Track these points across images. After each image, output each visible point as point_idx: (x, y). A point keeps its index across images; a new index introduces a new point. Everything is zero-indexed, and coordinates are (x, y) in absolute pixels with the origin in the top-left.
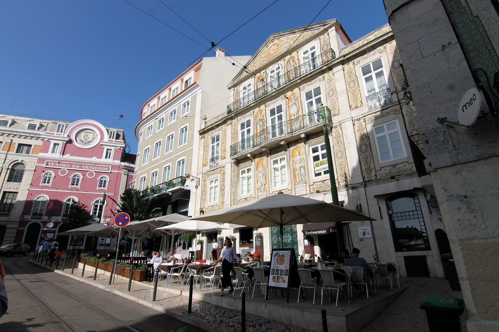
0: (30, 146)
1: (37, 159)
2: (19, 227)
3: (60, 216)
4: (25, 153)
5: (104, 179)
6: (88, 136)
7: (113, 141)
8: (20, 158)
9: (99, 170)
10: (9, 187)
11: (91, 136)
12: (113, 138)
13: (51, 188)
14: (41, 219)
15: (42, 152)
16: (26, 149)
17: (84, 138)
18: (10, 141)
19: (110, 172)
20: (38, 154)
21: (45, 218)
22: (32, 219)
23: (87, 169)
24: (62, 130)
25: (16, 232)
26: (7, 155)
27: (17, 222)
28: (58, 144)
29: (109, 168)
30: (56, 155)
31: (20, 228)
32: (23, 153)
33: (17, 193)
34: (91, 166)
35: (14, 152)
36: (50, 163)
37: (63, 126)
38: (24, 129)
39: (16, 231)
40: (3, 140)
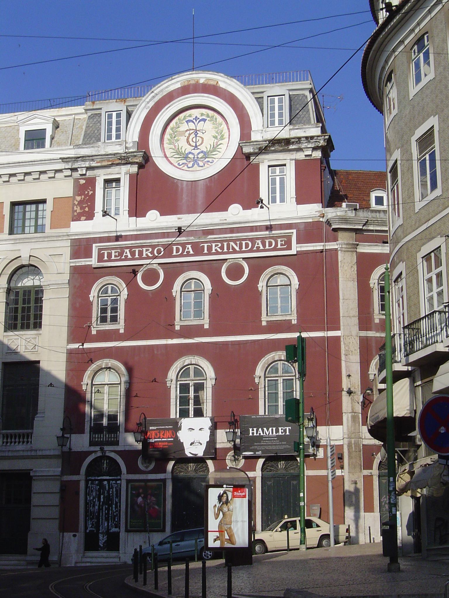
1: (68, 243)
2: (63, 473)
6: (200, 134)
9: (258, 250)
17: (188, 141)
19: (293, 252)
22: (92, 444)
23: (217, 253)
24: (118, 130)
25: (57, 490)
31: (66, 478)
32: (27, 230)
37: (119, 116)
38: (15, 148)
39: (56, 487)
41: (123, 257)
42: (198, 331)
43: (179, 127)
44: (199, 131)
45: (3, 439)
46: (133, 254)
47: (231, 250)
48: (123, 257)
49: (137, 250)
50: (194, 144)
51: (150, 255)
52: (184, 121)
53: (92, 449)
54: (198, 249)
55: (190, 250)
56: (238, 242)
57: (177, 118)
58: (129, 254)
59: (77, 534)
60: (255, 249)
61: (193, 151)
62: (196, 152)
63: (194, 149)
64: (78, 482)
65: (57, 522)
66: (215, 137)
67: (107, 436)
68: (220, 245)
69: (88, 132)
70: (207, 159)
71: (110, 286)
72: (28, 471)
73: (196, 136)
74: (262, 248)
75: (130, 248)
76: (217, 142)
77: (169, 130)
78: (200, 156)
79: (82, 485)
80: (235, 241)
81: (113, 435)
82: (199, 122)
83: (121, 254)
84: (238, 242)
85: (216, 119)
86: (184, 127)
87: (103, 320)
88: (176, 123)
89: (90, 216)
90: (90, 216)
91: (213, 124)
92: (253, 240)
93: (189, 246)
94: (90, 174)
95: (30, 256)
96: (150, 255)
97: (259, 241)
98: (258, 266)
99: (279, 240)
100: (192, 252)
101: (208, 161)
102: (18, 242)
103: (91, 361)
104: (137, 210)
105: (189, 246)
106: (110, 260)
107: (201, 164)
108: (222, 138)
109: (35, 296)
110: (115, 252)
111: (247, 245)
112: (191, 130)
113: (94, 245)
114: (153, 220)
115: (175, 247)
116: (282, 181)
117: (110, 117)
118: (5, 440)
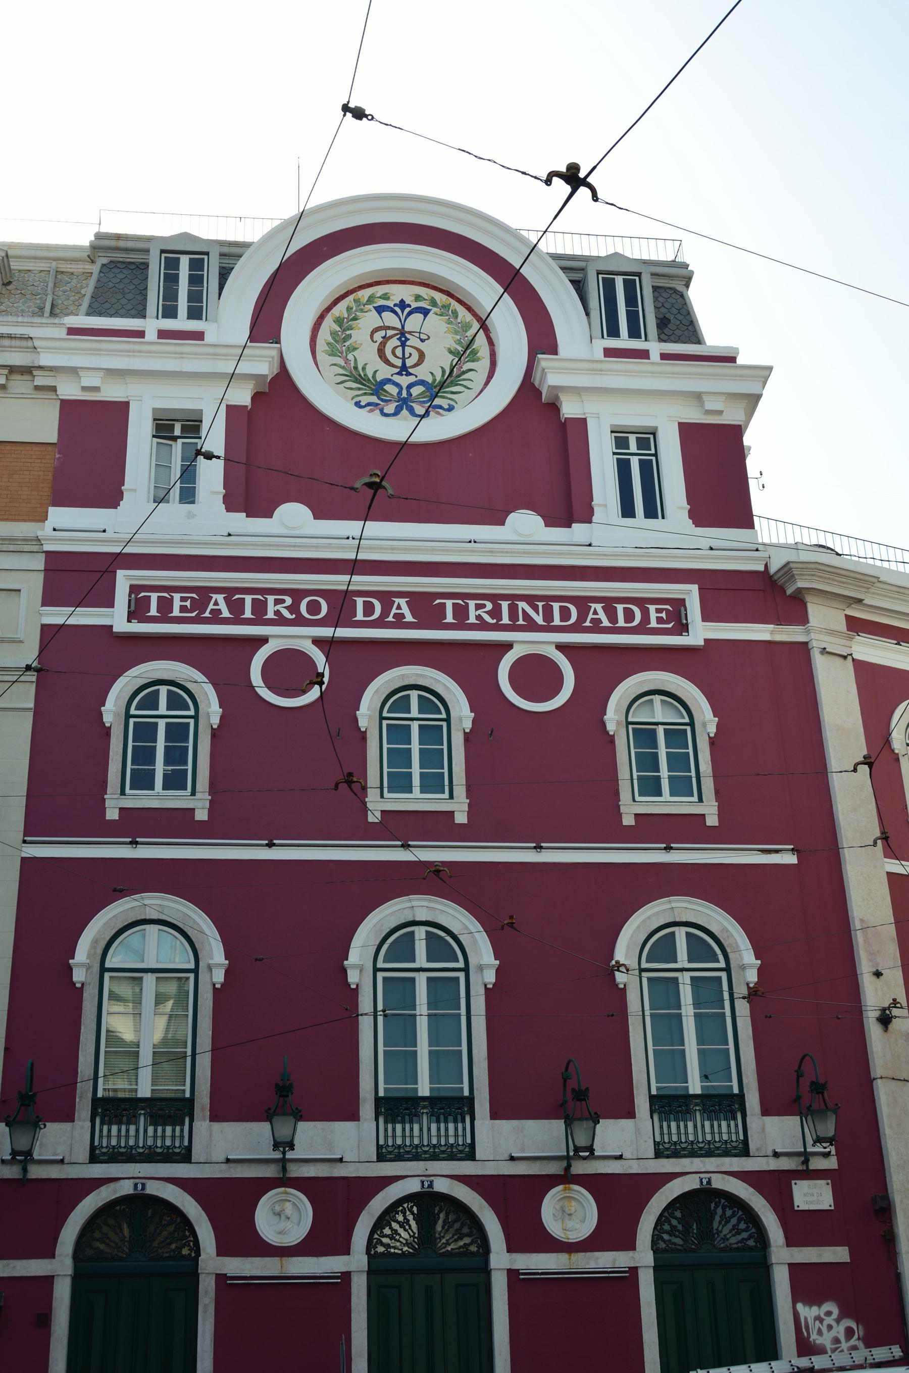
1: (39, 563)
5: (659, 713)
6: (413, 341)
9: (597, 627)
12: (634, 333)
13: (216, 828)
14: (186, 1156)
15: (66, 496)
20: (43, 518)
21: (226, 1145)
23: (482, 626)
28: (193, 426)
29: (679, 605)
30: (191, 515)
34: (513, 598)
36: (154, 597)
41: (207, 614)
42: (436, 826)
43: (355, 319)
44: (410, 333)
46: (236, 607)
48: (207, 614)
49: (248, 599)
50: (399, 363)
51: (286, 614)
52: (370, 307)
55: (406, 610)
57: (351, 298)
58: (223, 606)
60: (588, 624)
61: (397, 378)
62: (404, 381)
63: (400, 374)
64: (48, 1281)
67: (151, 1129)
68: (489, 606)
71: (163, 690)
73: (403, 345)
74: (606, 623)
75: (229, 592)
77: (328, 323)
78: (416, 391)
79: (62, 1292)
81: (160, 1129)
82: (410, 313)
85: (455, 314)
86: (370, 319)
87: (143, 781)
88: (349, 309)
89: (108, 494)
90: (108, 494)
91: (449, 322)
92: (583, 603)
93: (403, 602)
94: (112, 392)
96: (286, 614)
97: (599, 607)
98: (602, 667)
99: (652, 608)
100: (409, 618)
101: (441, 407)
103: (119, 893)
104: (250, 494)
105: (403, 602)
106: (165, 616)
107: (420, 410)
110: (183, 599)
112: (389, 328)
113: (121, 574)
114: (294, 526)
115: (360, 601)
116: (647, 469)
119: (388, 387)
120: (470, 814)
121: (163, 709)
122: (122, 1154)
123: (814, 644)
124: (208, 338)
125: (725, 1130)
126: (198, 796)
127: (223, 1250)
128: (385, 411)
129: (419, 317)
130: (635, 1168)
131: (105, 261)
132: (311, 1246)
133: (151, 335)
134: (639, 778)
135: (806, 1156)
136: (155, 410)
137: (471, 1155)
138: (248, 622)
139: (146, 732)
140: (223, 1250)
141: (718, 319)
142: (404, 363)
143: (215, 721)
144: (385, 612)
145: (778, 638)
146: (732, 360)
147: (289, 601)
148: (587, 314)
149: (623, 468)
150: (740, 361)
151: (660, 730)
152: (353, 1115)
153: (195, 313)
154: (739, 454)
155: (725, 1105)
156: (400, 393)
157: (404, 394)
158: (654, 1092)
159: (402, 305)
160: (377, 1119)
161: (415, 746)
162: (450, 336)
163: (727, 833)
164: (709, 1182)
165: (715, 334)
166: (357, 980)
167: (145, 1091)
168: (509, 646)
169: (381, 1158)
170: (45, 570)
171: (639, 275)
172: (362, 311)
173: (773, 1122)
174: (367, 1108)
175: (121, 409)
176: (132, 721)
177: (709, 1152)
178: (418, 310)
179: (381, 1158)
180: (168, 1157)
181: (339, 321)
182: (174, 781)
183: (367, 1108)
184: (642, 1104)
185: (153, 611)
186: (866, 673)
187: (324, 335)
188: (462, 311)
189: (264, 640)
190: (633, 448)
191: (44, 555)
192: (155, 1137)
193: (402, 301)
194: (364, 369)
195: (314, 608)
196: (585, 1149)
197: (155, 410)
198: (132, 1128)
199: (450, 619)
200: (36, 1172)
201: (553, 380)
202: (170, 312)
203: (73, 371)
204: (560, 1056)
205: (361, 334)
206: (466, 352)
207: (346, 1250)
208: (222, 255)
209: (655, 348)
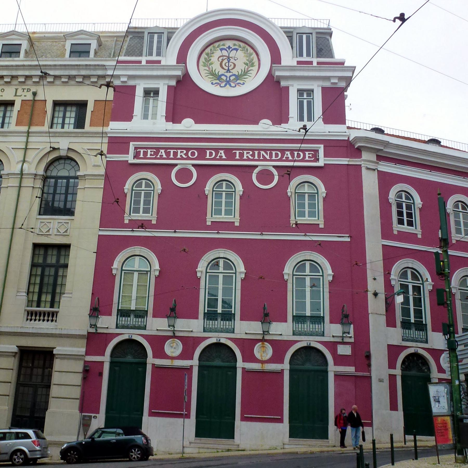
0: (81, 106)
1: (106, 140)
2: (87, 353)
3: (197, 318)
4: (72, 126)
5: (306, 189)
6: (232, 60)
7: (311, 63)
8: (64, 144)
9: (287, 160)
10: (44, 230)
11: (240, 58)
12: (308, 55)
14: (144, 328)
16: (73, 115)
18: (31, 98)
19: (321, 163)
21: (157, 325)
23: (248, 160)
26: (28, 136)
27: (80, 337)
28: (156, 92)
29: (316, 151)
30: (154, 124)
31: (89, 358)
33: (67, 247)
34: (259, 150)
35: (46, 128)
36: (142, 151)
39: (79, 366)
40: (16, 95)
41: (158, 157)
43: (213, 53)
45: (28, 315)
46: (168, 154)
47: (261, 158)
48: (158, 157)
49: (172, 151)
50: (227, 68)
51: (184, 156)
52: (218, 49)
53: (118, 331)
54: (230, 153)
56: (268, 152)
57: (212, 46)
59: (97, 415)
60: (284, 159)
62: (228, 74)
63: (227, 72)
64: (102, 363)
65: (78, 401)
66: (246, 64)
68: (251, 153)
69: (129, 50)
70: (238, 81)
71: (144, 181)
72: (51, 350)
73: (229, 62)
74: (290, 158)
75: (166, 149)
76: (248, 69)
77: (204, 55)
78: (232, 78)
80: (265, 150)
83: (156, 153)
84: (268, 152)
85: (247, 50)
87: (137, 211)
88: (211, 50)
89: (128, 117)
90: (128, 117)
91: (245, 53)
92: (283, 151)
93: (222, 152)
94: (131, 83)
95: (69, 149)
96: (184, 156)
98: (288, 173)
99: (307, 153)
100: (224, 157)
102: (57, 135)
104: (173, 116)
105: (222, 152)
106: (145, 157)
107: (233, 85)
108: (252, 65)
109: (70, 186)
110: (151, 152)
111: (277, 155)
113: (131, 143)
114: (188, 126)
117: (152, 38)
118: (29, 317)
119: (223, 77)
120: (240, 222)
121: (143, 188)
122: (126, 326)
123: (363, 165)
124: (163, 63)
125: (317, 327)
126: (153, 216)
127: (154, 357)
128: (221, 85)
129: (235, 51)
130: (286, 338)
131: (131, 36)
132: (182, 357)
133: (144, 63)
134: (298, 211)
135: (343, 337)
136: (144, 88)
137: (234, 333)
138: (172, 159)
139: (138, 195)
140: (154, 357)
141: (341, 49)
142: (228, 68)
143: (160, 191)
144: (216, 155)
145: (350, 163)
146: (343, 63)
147: (185, 152)
148: (292, 48)
149: (301, 105)
150: (346, 65)
151: (307, 195)
152: (197, 318)
153: (159, 54)
154: (343, 98)
155: (317, 319)
156: (227, 79)
157: (228, 79)
158: (294, 314)
159: (229, 47)
160: (204, 319)
161: (224, 200)
162: (245, 58)
163: (326, 230)
164: (310, 344)
165: (338, 55)
166: (200, 275)
167: (133, 308)
168: (256, 166)
169: (204, 331)
170: (108, 143)
171: (312, 34)
172: (215, 50)
173: (333, 325)
174: (201, 315)
175: (134, 88)
176: (134, 191)
177: (311, 334)
178: (235, 49)
179: (204, 331)
180: (139, 328)
181: (207, 54)
182: (146, 211)
183: (201, 315)
184: (290, 318)
185: (142, 156)
186: (381, 175)
187: (202, 59)
188: (249, 49)
189: (176, 165)
190: (305, 96)
191: (108, 138)
192: (136, 322)
193: (229, 46)
194: (215, 71)
195: (193, 154)
196: (266, 332)
197: (144, 88)
198: (129, 318)
199: (237, 157)
200: (100, 331)
201: (277, 73)
202: (151, 54)
203: (118, 77)
204: (264, 301)
205: (214, 59)
206: (250, 64)
207: (192, 359)
208: (169, 33)
209: (315, 61)
